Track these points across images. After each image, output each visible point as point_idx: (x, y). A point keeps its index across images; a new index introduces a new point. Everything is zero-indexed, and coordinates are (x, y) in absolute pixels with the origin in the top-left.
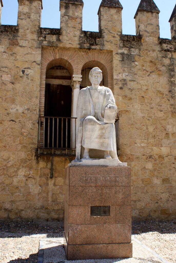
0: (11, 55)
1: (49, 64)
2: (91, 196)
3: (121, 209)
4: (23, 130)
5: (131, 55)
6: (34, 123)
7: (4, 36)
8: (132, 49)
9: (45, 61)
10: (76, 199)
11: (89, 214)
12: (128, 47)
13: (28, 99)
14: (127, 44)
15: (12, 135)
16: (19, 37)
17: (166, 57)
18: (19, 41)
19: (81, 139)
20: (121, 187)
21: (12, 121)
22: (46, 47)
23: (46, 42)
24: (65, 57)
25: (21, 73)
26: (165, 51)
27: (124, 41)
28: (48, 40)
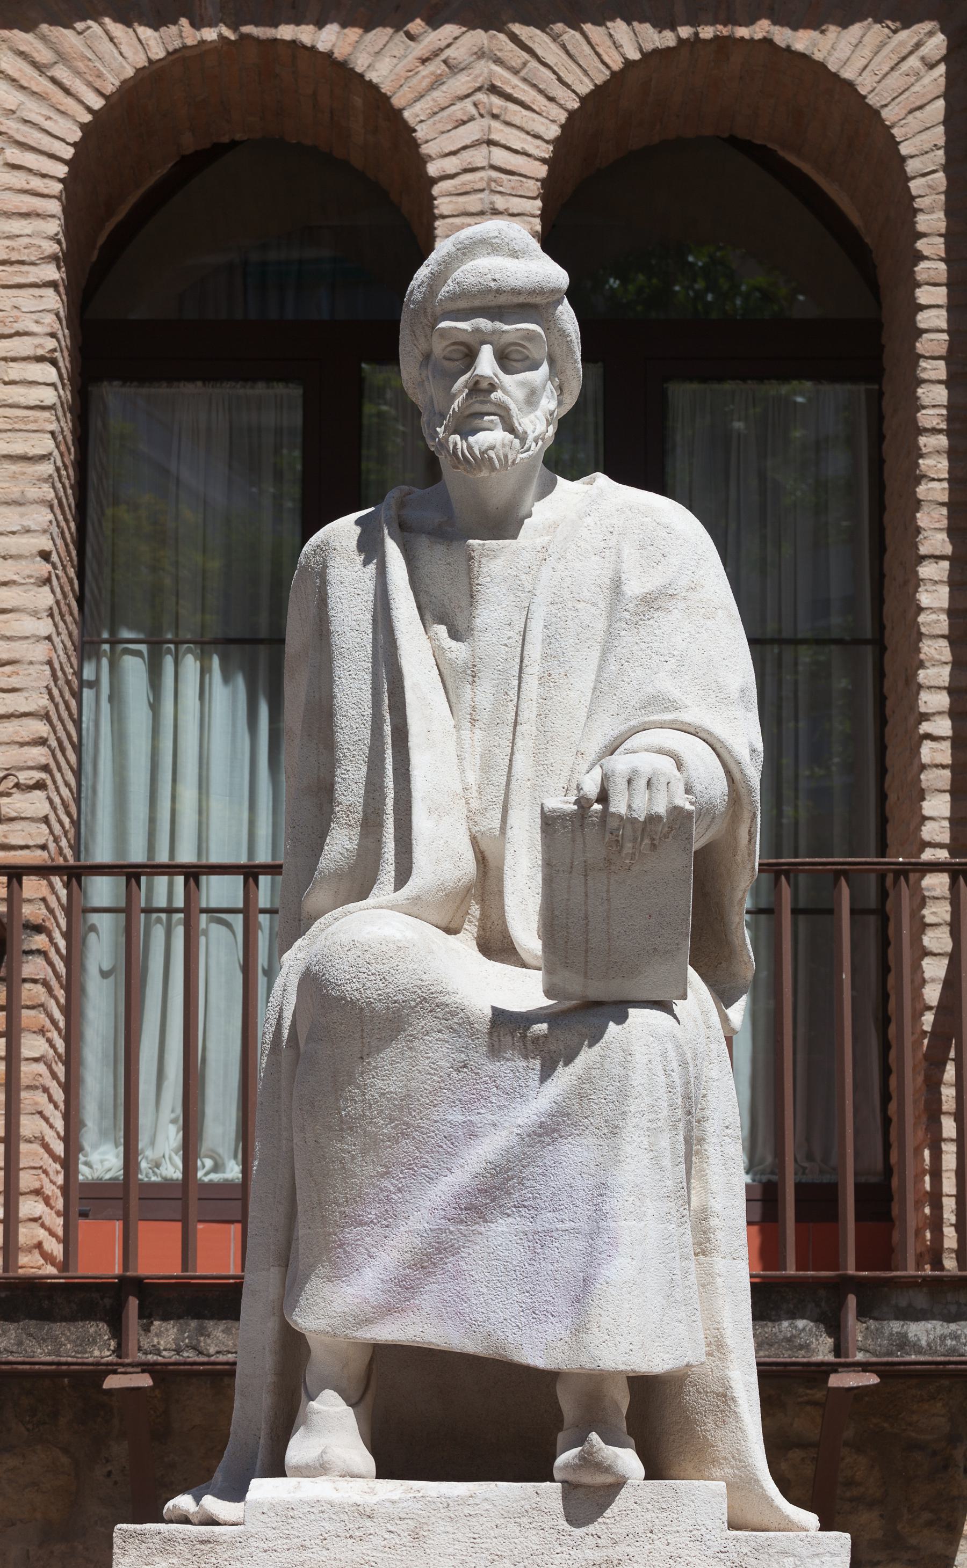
1: (96, 134)
9: (41, 84)
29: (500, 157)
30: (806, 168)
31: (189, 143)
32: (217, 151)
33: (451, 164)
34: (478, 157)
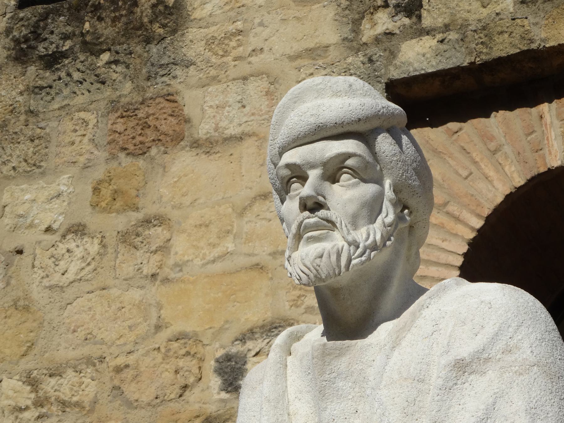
0: (127, 238)
7: (66, 92)
16: (189, 64)
18: (192, 100)
23: (428, 43)
25: (215, 382)
28: (440, 22)
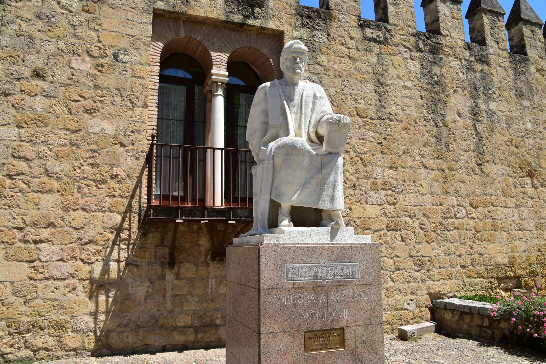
2: (306, 308)
3: (365, 334)
4: (115, 168)
5: (315, 43)
6: (137, 156)
8: (315, 33)
10: (274, 318)
11: (303, 349)
12: (309, 28)
13: (125, 110)
14: (308, 22)
15: (91, 180)
17: (368, 50)
19: (269, 186)
20: (364, 286)
21: (91, 152)
22: (161, 12)
24: (197, 36)
25: (112, 57)
26: (370, 40)
27: (302, 16)
29: (221, 57)
30: (253, 67)
31: (173, 52)
32: (176, 54)
33: (215, 58)
34: (218, 57)
